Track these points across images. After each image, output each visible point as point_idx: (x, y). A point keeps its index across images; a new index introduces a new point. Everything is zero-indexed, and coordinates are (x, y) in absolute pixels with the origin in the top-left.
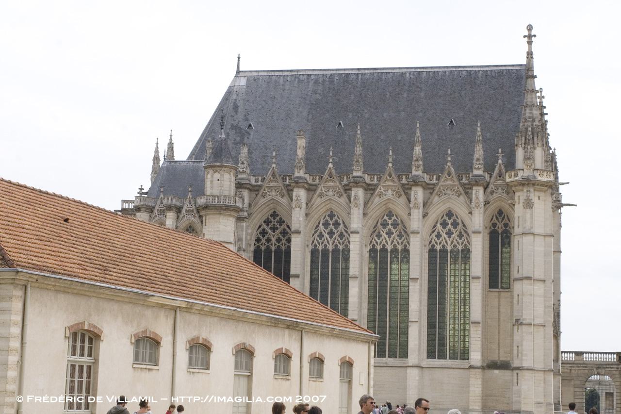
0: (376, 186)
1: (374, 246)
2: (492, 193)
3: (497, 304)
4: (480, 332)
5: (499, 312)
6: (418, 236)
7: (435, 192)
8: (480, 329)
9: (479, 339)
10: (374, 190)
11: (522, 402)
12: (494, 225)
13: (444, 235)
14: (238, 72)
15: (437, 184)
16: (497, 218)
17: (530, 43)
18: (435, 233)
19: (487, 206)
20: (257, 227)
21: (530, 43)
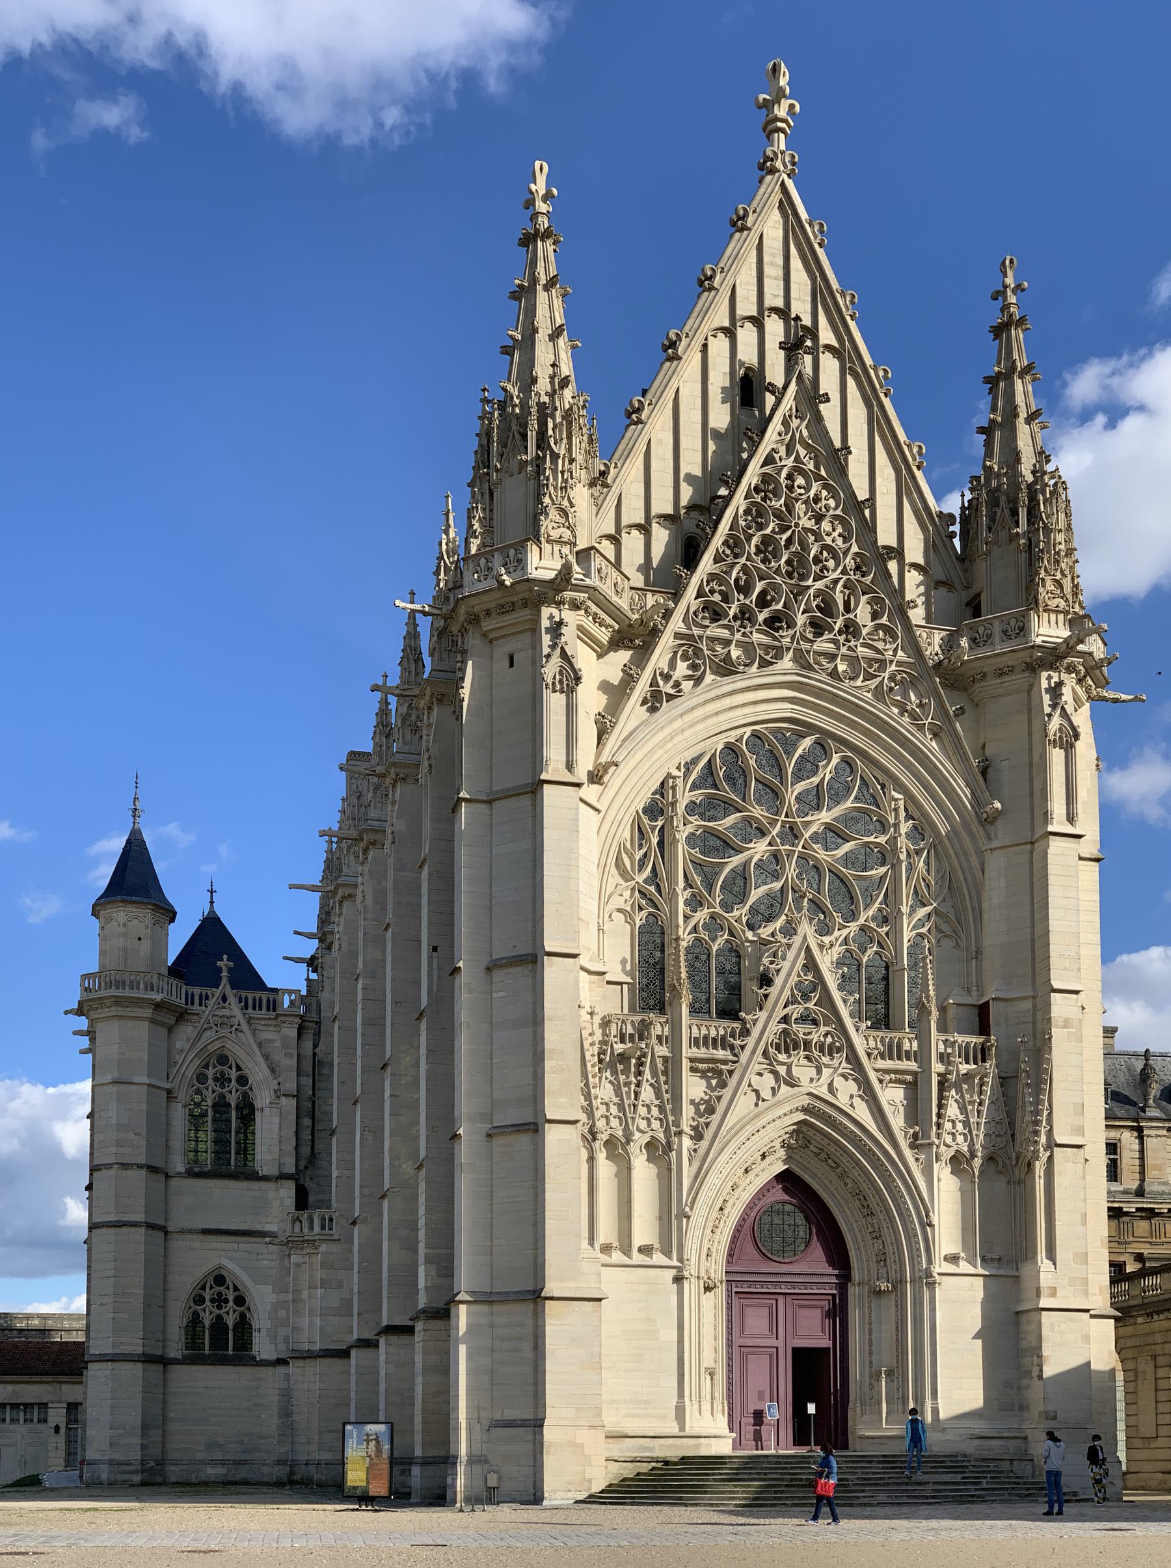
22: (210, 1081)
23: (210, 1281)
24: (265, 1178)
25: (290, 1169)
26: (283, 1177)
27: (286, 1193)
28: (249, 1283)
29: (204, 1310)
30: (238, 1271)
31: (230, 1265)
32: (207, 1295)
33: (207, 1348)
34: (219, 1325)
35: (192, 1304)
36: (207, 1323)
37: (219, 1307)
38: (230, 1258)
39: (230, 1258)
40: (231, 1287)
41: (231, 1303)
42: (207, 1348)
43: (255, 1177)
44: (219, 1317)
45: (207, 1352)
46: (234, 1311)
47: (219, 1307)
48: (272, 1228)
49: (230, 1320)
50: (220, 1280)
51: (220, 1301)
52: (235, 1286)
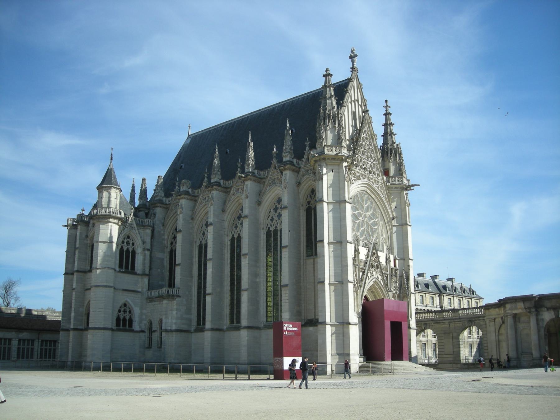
0: (231, 188)
1: (233, 235)
2: (303, 175)
3: (313, 269)
4: (287, 295)
5: (314, 276)
6: (248, 220)
7: (266, 183)
8: (288, 292)
9: (288, 301)
10: (229, 192)
11: (319, 355)
12: (309, 203)
13: (276, 218)
14: (189, 136)
15: (267, 177)
16: (311, 196)
17: (353, 62)
18: (270, 218)
19: (301, 187)
20: (171, 233)
21: (353, 62)
24: (139, 275)
25: (147, 272)
26: (144, 274)
27: (146, 280)
28: (133, 306)
30: (131, 303)
31: (129, 300)
32: (122, 310)
34: (124, 319)
38: (129, 299)
39: (129, 299)
43: (135, 274)
48: (140, 290)
49: (128, 318)
50: (125, 305)
51: (125, 312)
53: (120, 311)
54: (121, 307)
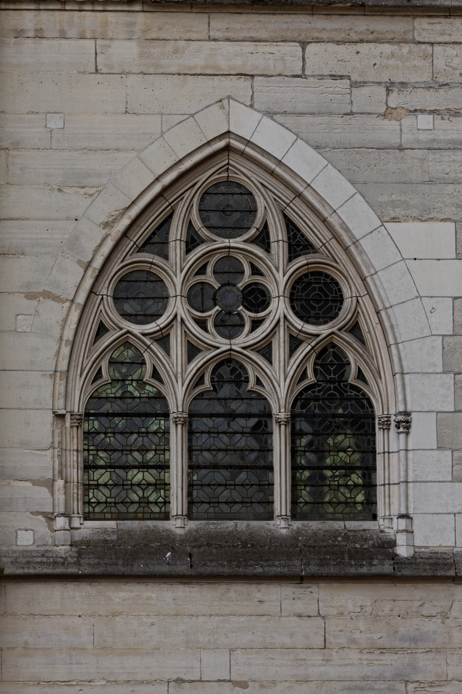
22: (178, 307)
23: (186, 213)
29: (163, 339)
30: (303, 163)
31: (271, 138)
32: (176, 269)
33: (177, 503)
35: (111, 314)
36: (177, 397)
37: (228, 325)
40: (277, 233)
41: (279, 307)
42: (177, 504)
44: (229, 370)
45: (176, 526)
46: (294, 343)
47: (228, 325)
52: (291, 226)
53: (137, 291)
54: (149, 230)
